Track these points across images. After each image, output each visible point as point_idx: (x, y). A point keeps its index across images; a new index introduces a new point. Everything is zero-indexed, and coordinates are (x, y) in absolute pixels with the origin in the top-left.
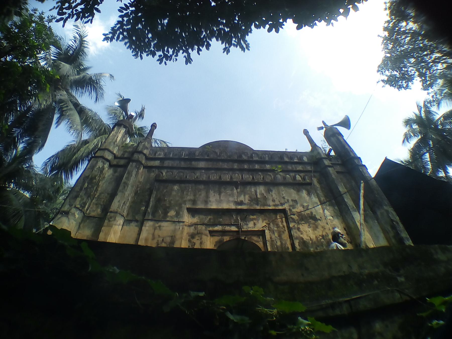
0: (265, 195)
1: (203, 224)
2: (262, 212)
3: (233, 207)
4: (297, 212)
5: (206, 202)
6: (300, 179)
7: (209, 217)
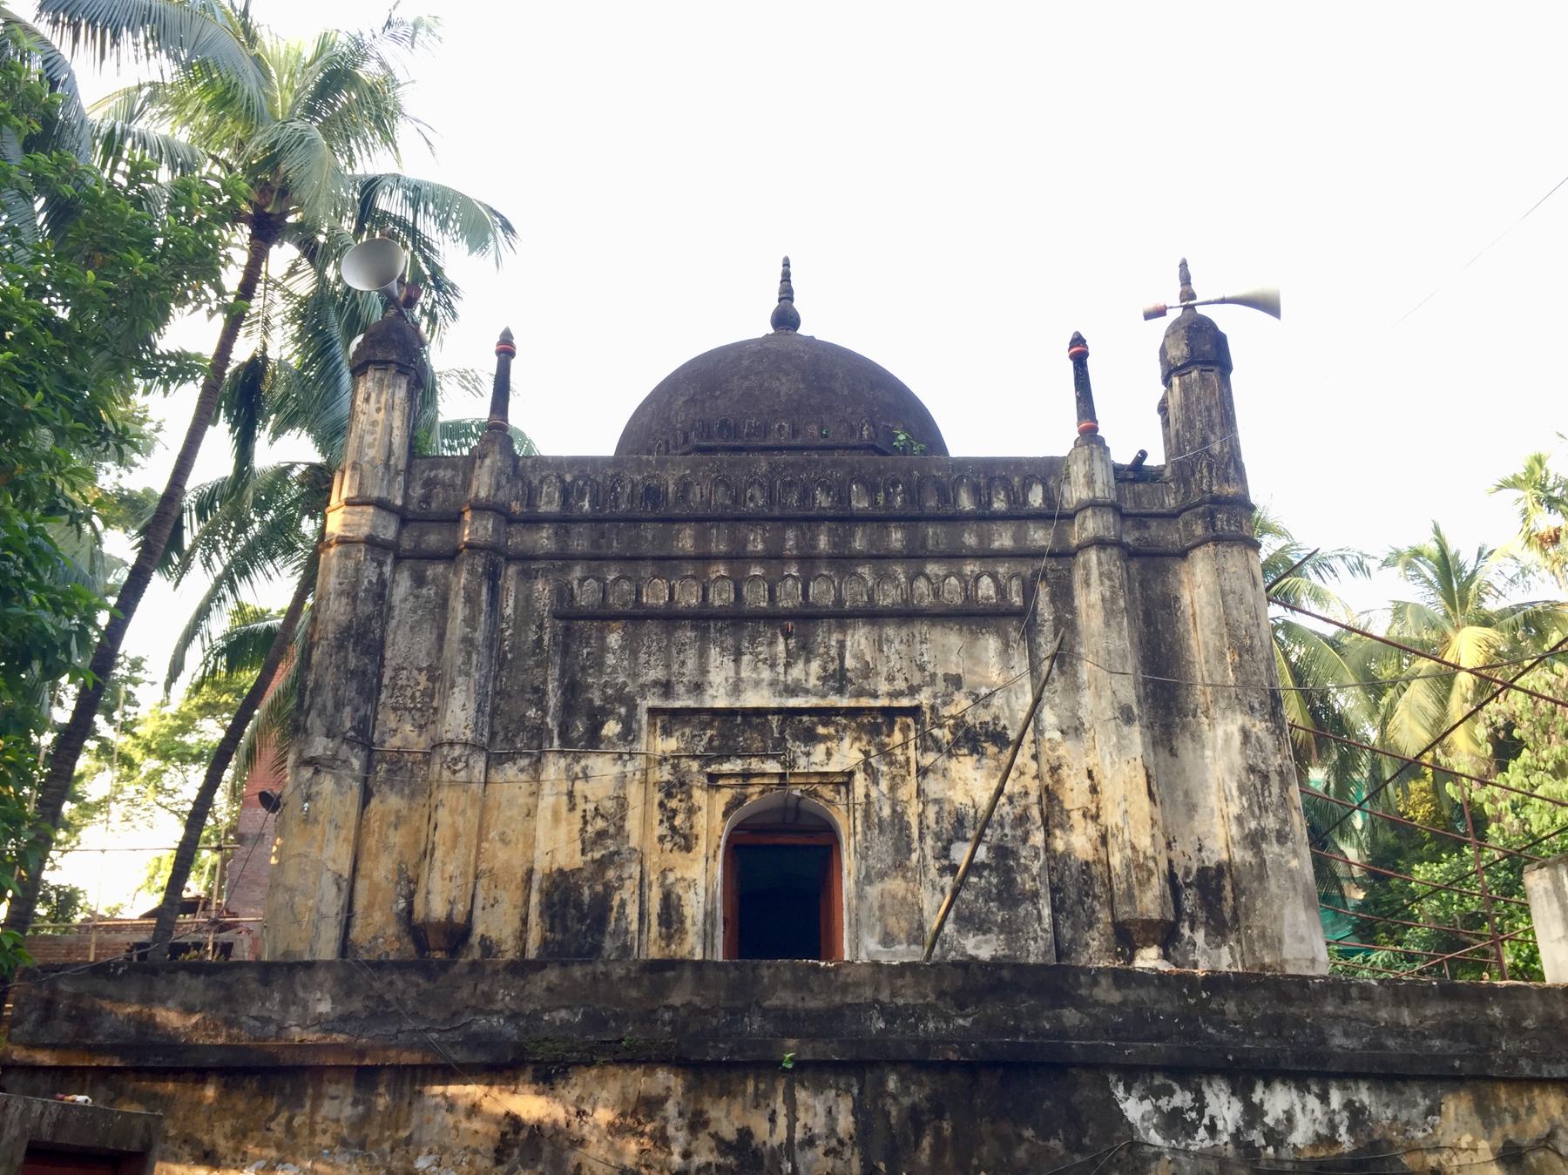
0: (868, 658)
1: (695, 757)
3: (774, 703)
4: (951, 717)
5: (698, 688)
6: (992, 593)
7: (709, 733)
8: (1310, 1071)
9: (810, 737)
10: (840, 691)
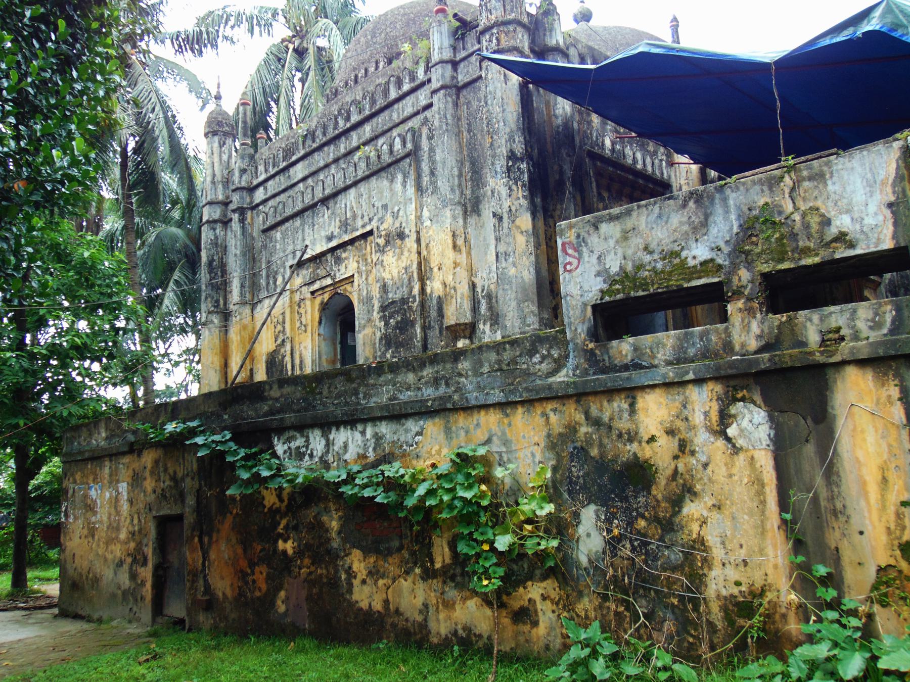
1: (305, 285)
2: (352, 242)
9: (338, 261)
10: (346, 232)
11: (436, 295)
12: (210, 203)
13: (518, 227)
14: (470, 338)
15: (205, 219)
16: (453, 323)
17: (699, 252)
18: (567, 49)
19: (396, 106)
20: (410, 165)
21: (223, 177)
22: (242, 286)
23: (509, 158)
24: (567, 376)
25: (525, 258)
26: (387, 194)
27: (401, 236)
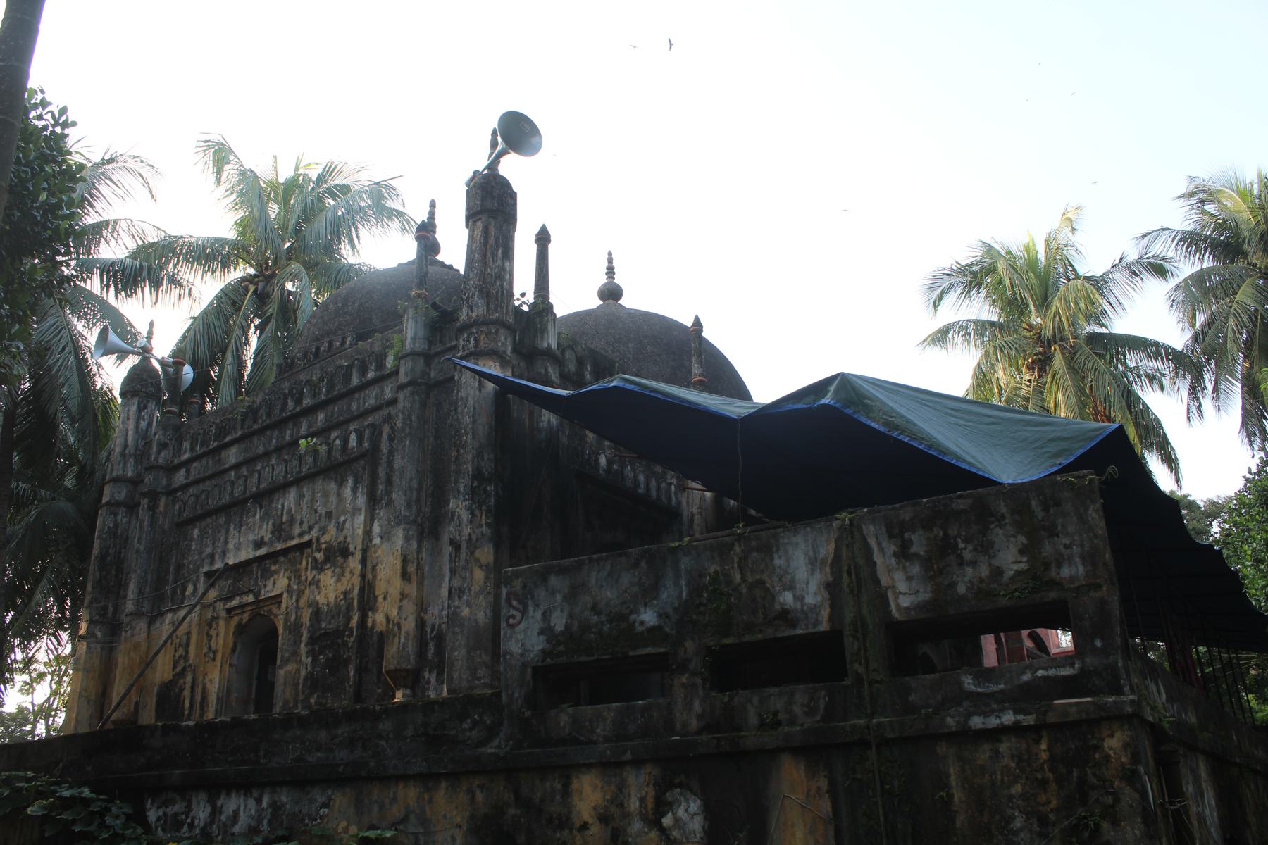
1: (221, 600)
5: (224, 553)
8: (245, 785)
9: (267, 574)
10: (279, 539)
11: (378, 629)
12: (116, 480)
13: (477, 560)
14: (413, 688)
15: (105, 499)
16: (392, 667)
17: (648, 617)
18: (563, 352)
19: (357, 395)
20: (364, 469)
21: (137, 448)
22: (140, 592)
23: (474, 477)
24: (499, 747)
25: (481, 597)
26: (333, 498)
27: (345, 552)
